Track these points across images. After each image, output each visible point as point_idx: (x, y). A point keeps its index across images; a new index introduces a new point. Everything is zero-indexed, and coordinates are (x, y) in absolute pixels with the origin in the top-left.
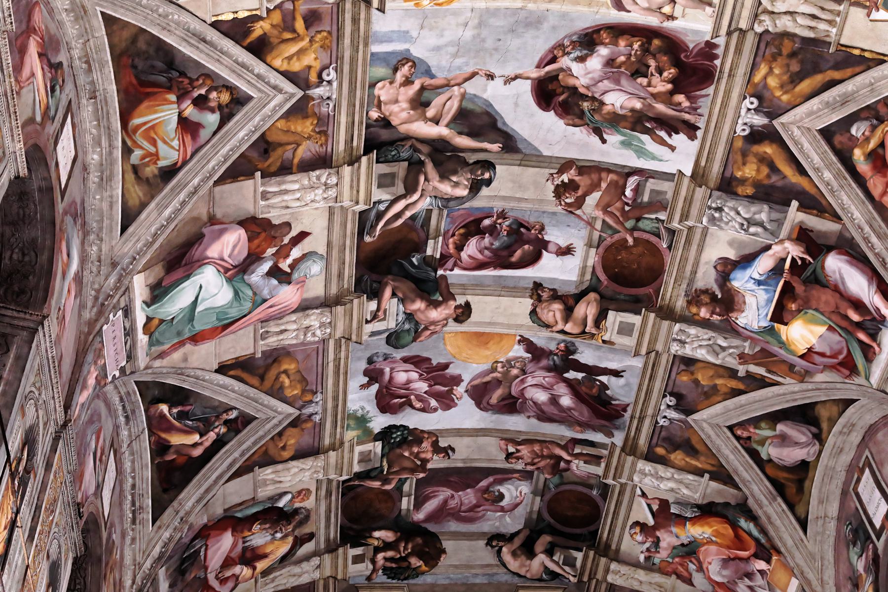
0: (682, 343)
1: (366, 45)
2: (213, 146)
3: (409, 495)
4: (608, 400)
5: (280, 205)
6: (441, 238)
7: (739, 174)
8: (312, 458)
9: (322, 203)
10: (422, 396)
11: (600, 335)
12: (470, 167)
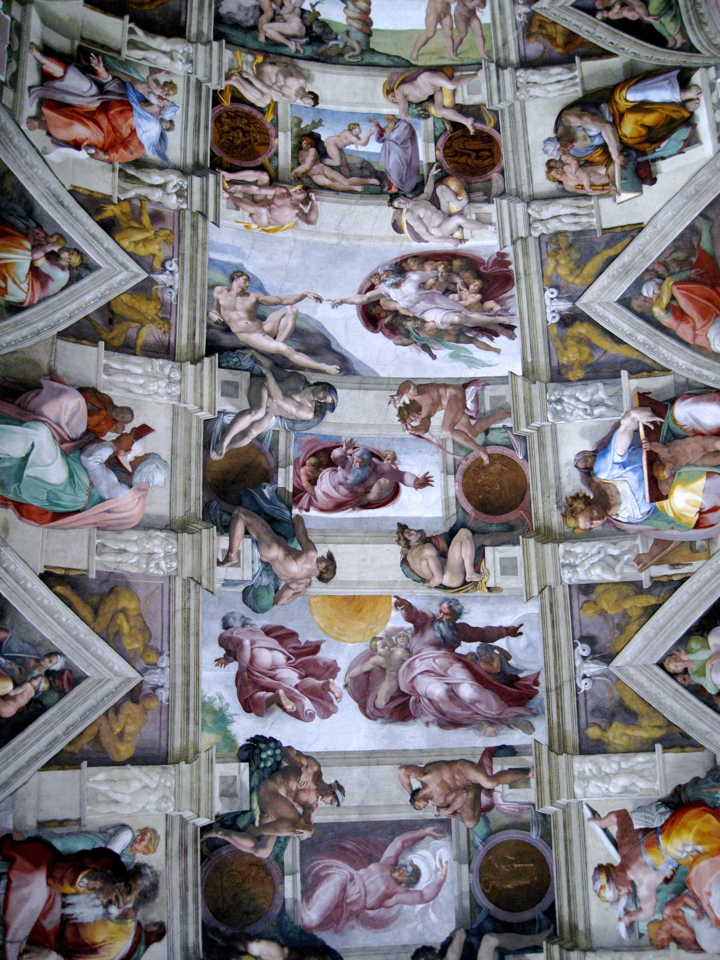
0: (573, 567)
1: (204, 249)
2: (59, 300)
3: (293, 873)
4: (514, 673)
5: (121, 385)
6: (291, 468)
7: (564, 361)
8: (158, 768)
9: (165, 398)
10: (293, 692)
11: (483, 581)
12: (312, 388)
